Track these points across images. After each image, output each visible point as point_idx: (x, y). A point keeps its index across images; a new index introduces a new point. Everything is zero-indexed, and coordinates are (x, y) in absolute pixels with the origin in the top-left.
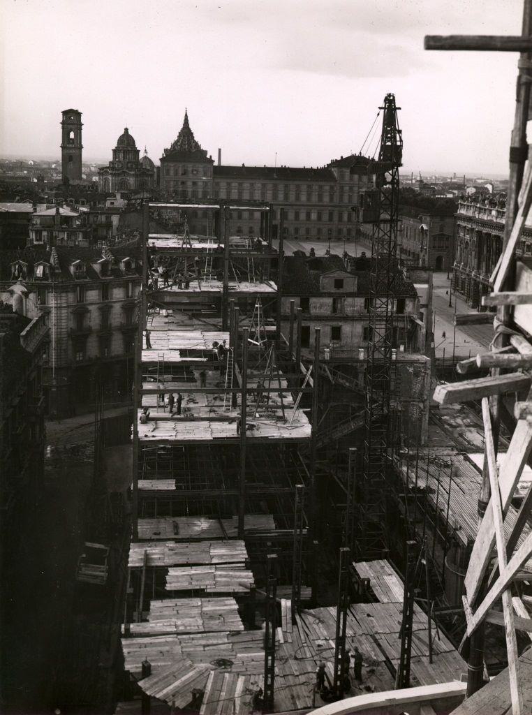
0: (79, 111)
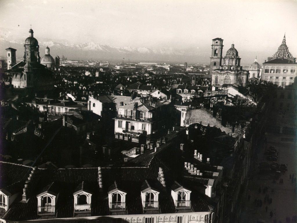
0: (222, 39)
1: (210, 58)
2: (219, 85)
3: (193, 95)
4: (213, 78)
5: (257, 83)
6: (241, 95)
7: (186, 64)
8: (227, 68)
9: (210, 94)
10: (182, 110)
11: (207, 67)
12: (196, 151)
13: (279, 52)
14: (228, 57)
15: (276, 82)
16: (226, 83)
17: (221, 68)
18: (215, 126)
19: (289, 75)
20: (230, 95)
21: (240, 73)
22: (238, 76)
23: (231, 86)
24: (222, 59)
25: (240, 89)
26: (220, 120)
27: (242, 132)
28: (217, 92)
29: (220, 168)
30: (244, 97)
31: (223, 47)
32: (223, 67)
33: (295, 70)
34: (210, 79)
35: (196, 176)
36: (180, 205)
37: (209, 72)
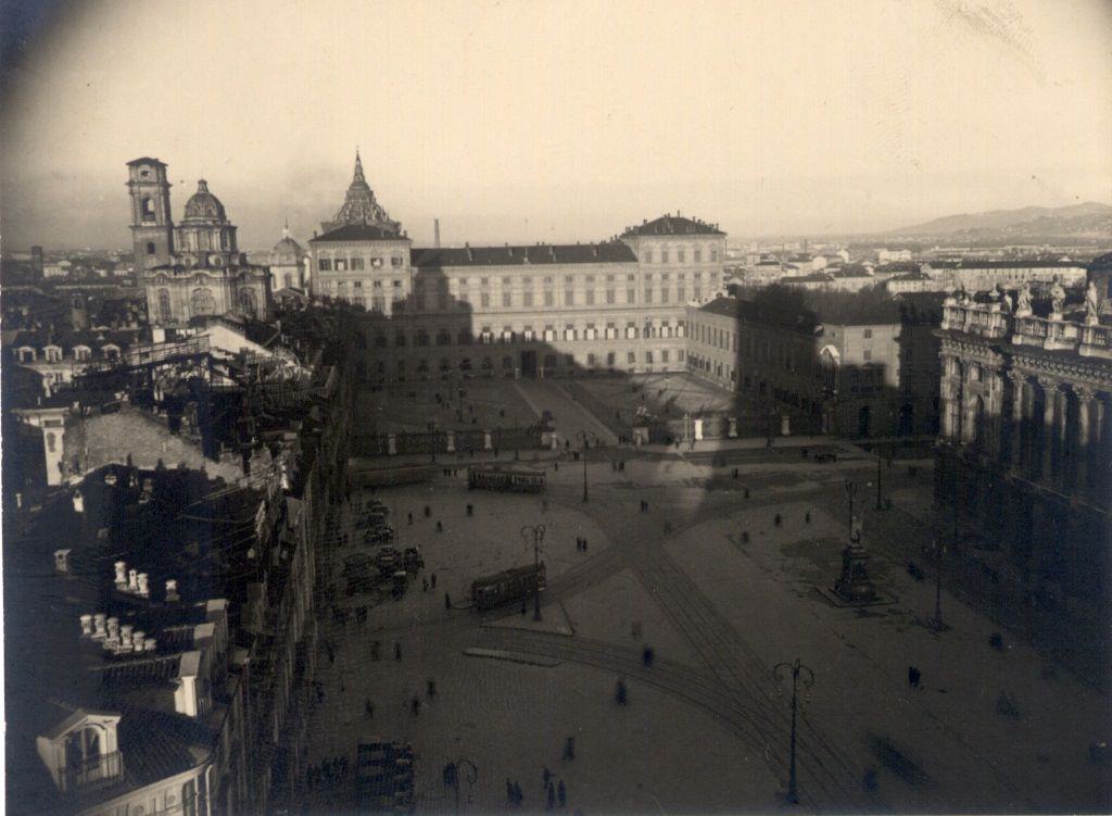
0: (161, 160)
1: (131, 227)
2: (176, 321)
3: (84, 366)
4: (153, 300)
5: (301, 305)
6: (258, 349)
7: (37, 250)
8: (194, 261)
9: (146, 355)
10: (48, 424)
11: (125, 259)
12: (119, 565)
13: (350, 206)
14: (193, 224)
15: (356, 299)
16: (200, 312)
17: (174, 262)
18: (184, 465)
19: (388, 275)
20: (220, 351)
21: (242, 275)
22: (236, 285)
23: (219, 322)
24: (174, 231)
25: (252, 330)
26: (195, 443)
27: (275, 468)
28: (173, 345)
29: (217, 605)
30: (268, 354)
31: (171, 190)
32: (182, 257)
33: (402, 259)
34: (142, 303)
35: (133, 655)
36: (82, 778)
37: (133, 276)
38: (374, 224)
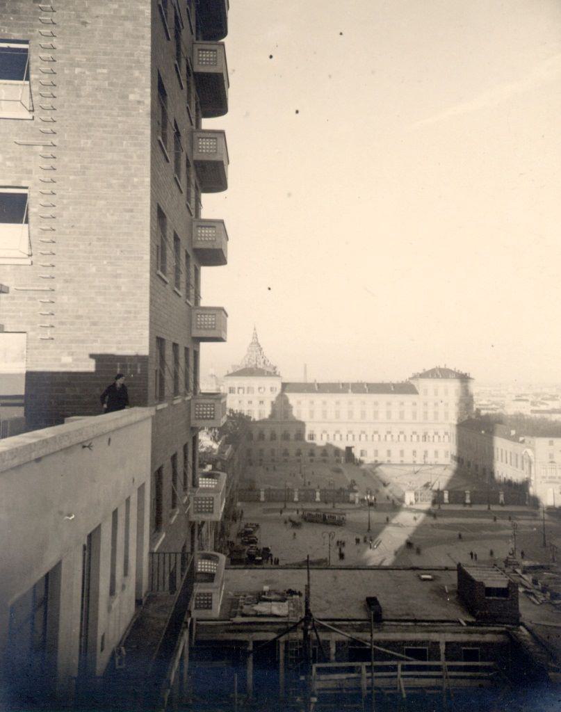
13: (248, 356)
15: (249, 411)
38: (262, 367)
